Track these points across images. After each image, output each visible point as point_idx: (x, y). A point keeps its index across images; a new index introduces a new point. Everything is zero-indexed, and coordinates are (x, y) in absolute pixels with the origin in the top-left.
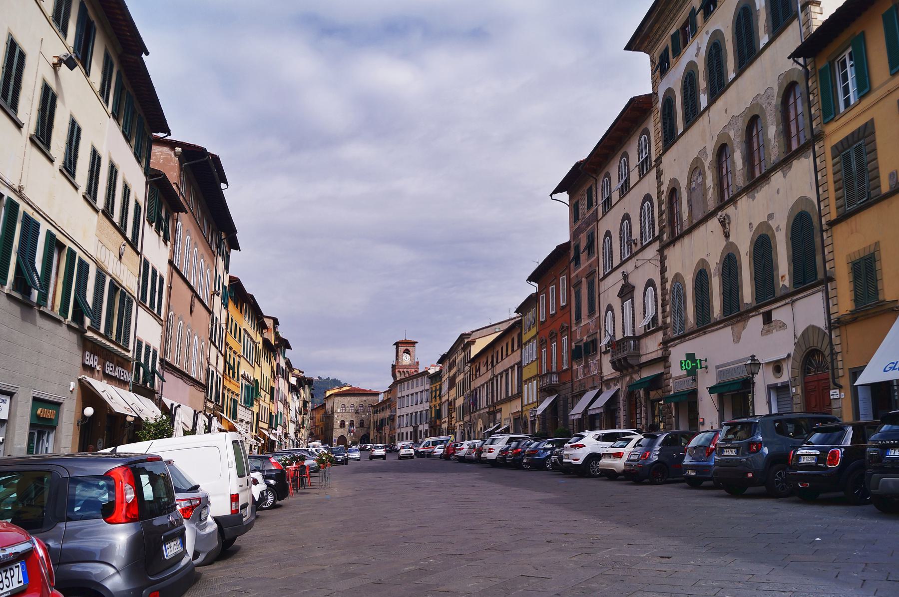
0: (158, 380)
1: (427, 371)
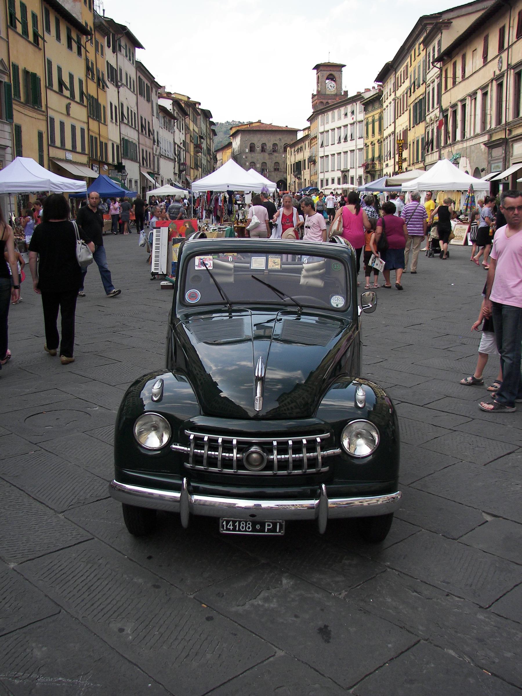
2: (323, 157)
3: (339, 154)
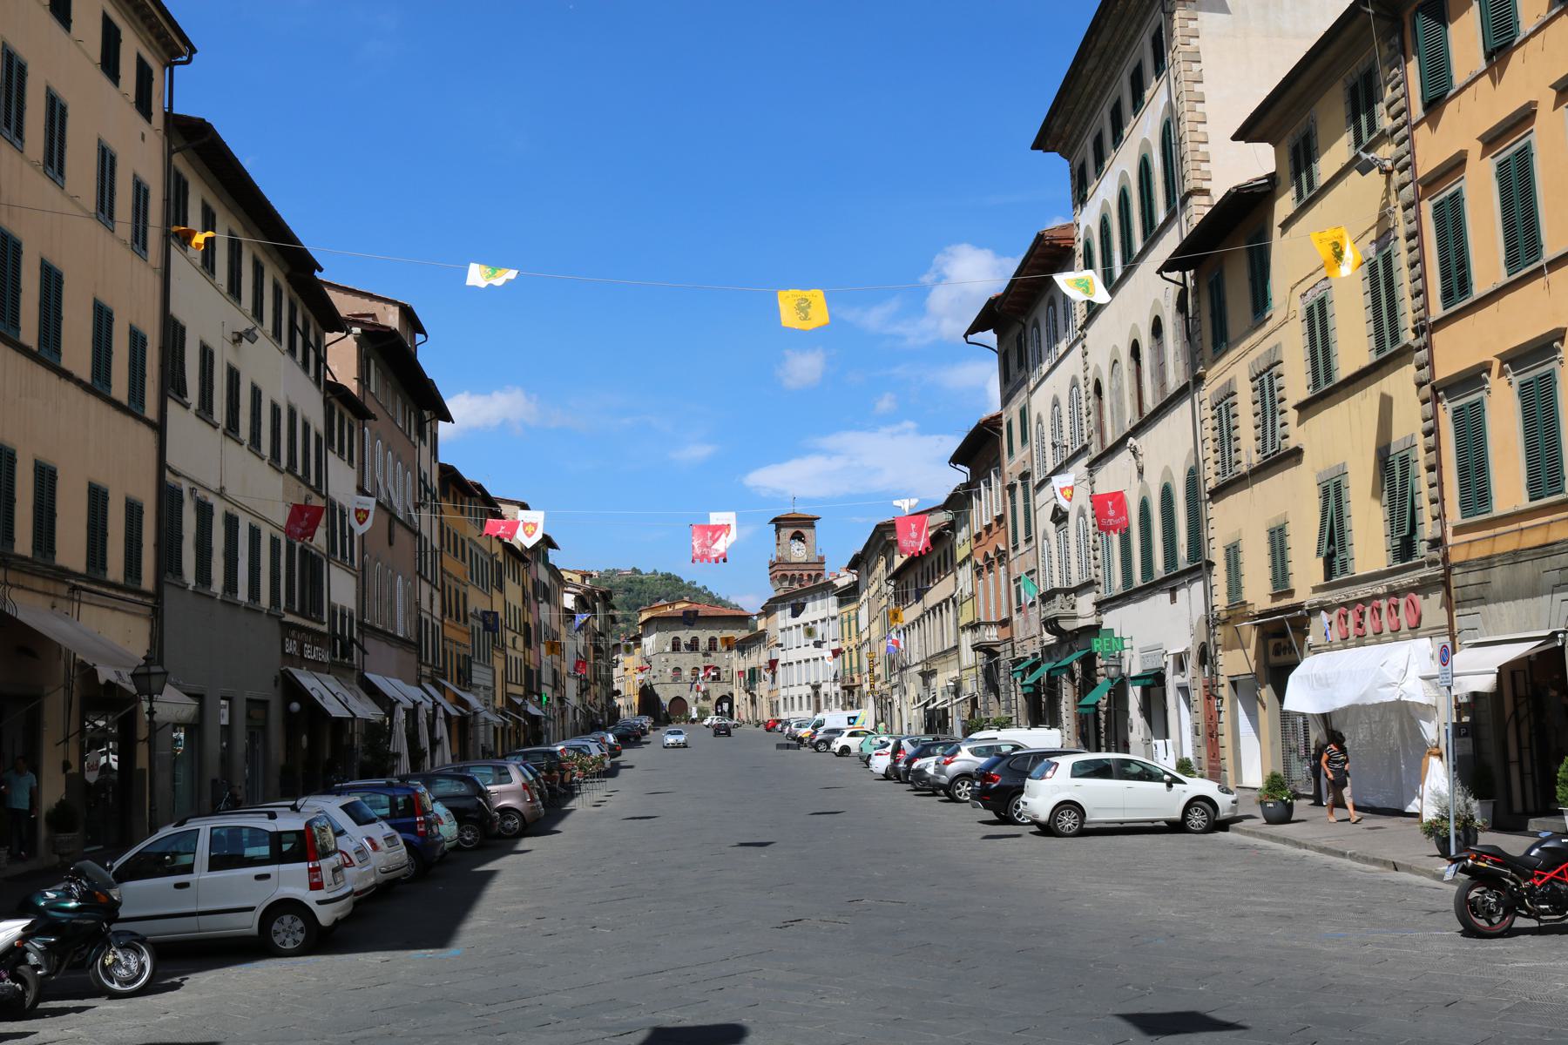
0: (358, 654)
1: (831, 582)
2: (785, 664)
3: (807, 661)
